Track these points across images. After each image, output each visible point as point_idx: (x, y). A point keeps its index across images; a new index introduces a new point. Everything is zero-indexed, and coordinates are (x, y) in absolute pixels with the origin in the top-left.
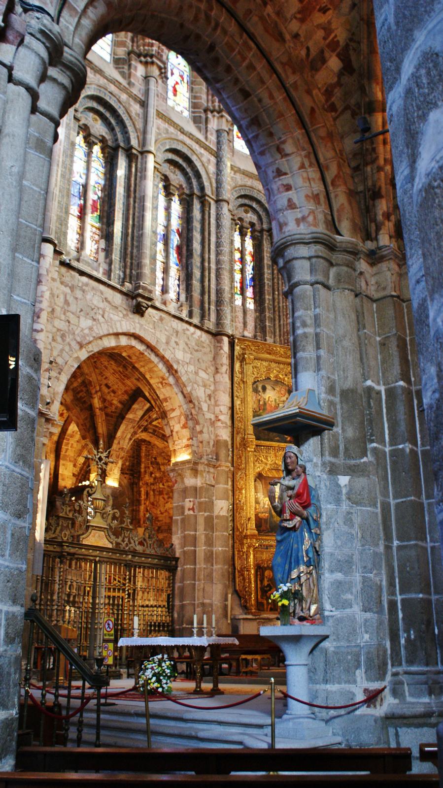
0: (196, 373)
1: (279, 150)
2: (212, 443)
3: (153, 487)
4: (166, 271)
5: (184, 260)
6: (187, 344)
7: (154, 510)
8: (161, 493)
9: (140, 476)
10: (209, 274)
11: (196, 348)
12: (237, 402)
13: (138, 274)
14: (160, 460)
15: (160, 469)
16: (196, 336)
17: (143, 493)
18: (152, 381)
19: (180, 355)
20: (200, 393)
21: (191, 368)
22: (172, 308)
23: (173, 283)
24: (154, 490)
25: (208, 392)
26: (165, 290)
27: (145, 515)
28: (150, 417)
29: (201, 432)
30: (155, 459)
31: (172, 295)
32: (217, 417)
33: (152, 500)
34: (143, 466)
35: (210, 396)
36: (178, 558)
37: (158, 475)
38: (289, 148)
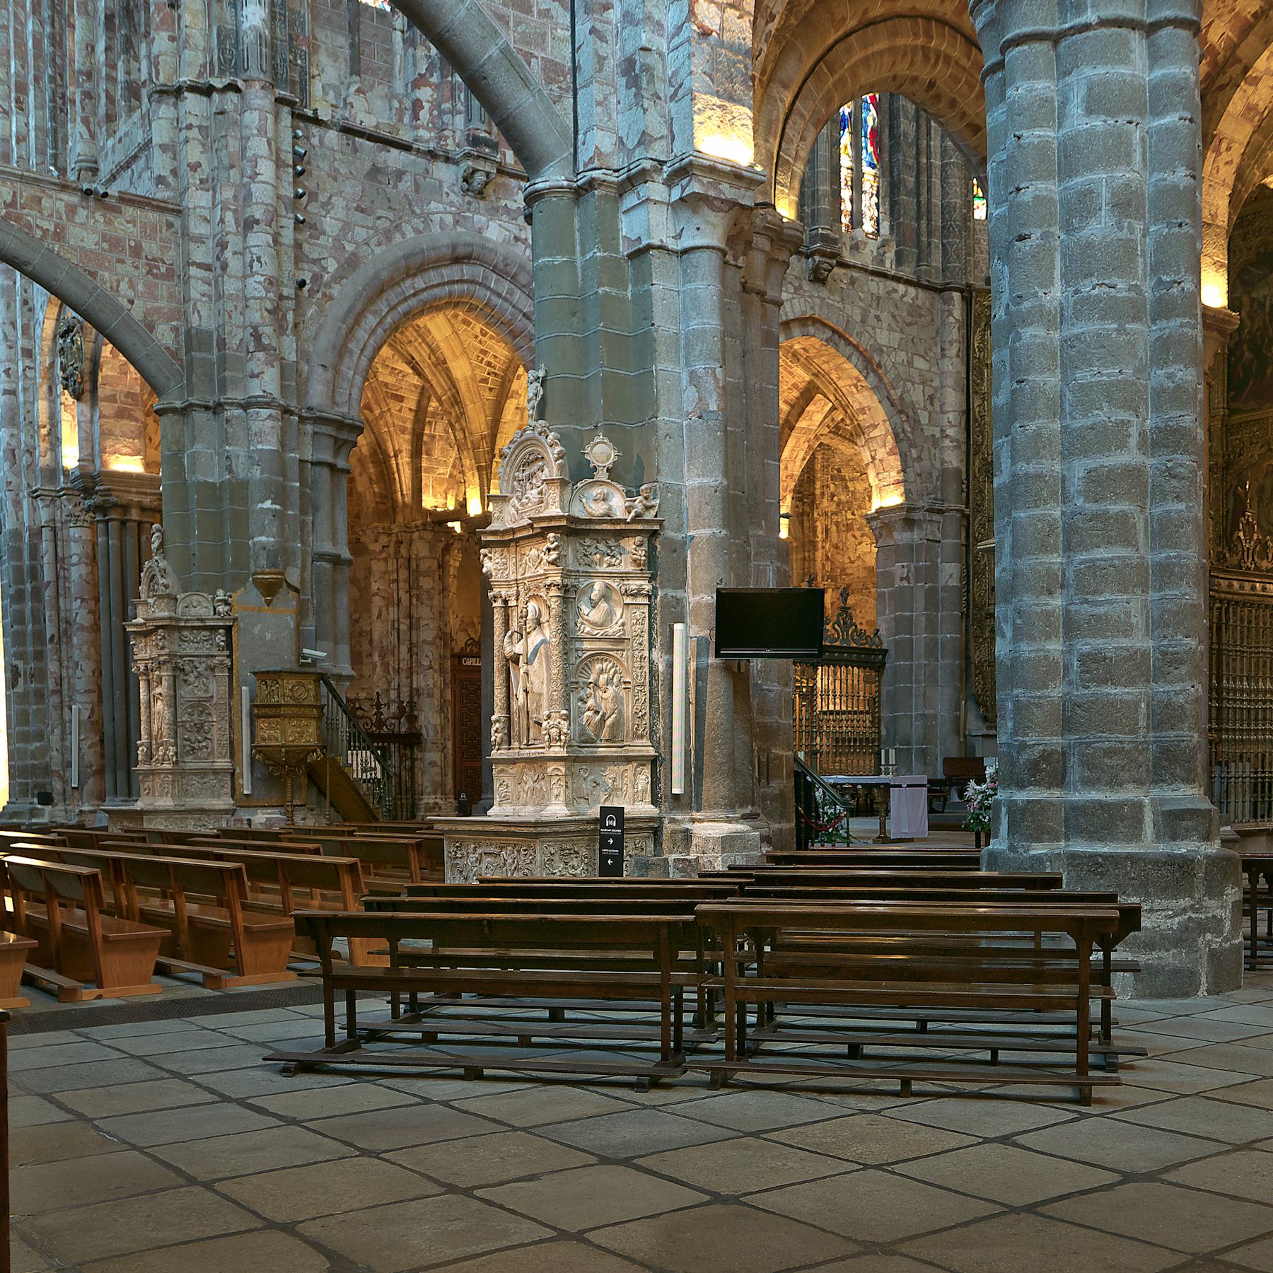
0: (910, 363)
2: (935, 474)
3: (835, 518)
4: (857, 184)
5: (886, 157)
6: (894, 317)
7: (839, 557)
8: (849, 527)
9: (813, 501)
10: (929, 177)
11: (909, 320)
12: (976, 402)
13: (813, 211)
14: (846, 473)
15: (847, 487)
16: (908, 299)
17: (819, 529)
18: (840, 384)
19: (883, 337)
20: (917, 395)
21: (902, 356)
22: (866, 258)
23: (869, 205)
24: (837, 524)
25: (929, 391)
26: (856, 221)
27: (824, 566)
28: (833, 420)
29: (919, 459)
30: (839, 471)
31: (868, 226)
32: (942, 431)
33: (835, 539)
34: (818, 485)
35: (931, 398)
36: (886, 651)
37: (843, 498)
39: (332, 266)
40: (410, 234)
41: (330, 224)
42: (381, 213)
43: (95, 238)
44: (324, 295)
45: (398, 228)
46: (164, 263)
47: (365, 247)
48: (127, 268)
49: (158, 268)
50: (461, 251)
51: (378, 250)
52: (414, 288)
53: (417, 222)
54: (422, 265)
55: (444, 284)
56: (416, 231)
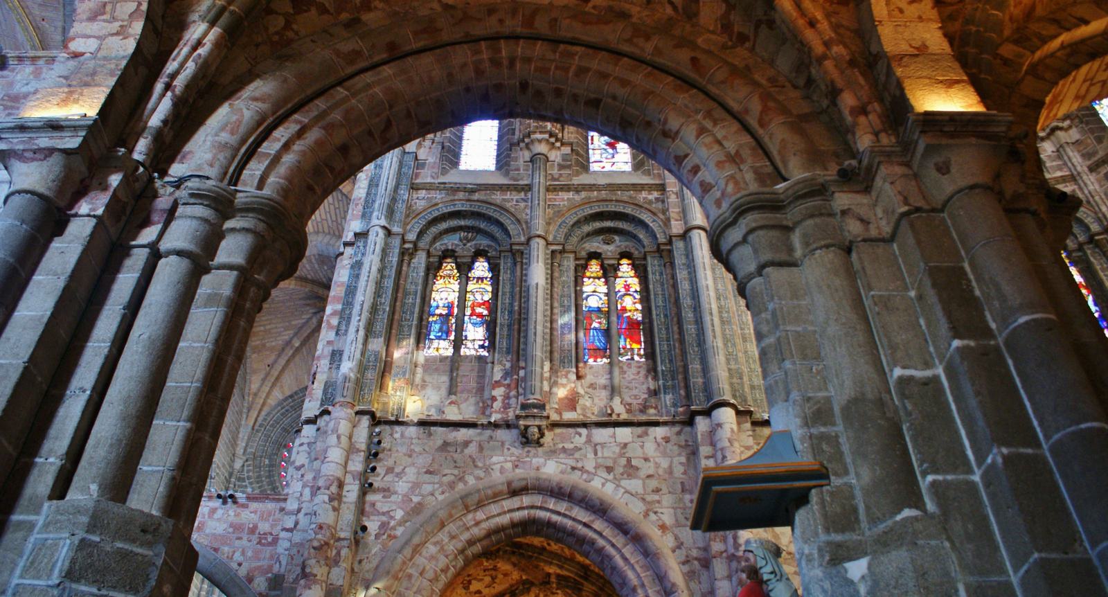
1: (666, 134)
38: (674, 123)
39: (399, 514)
40: (471, 481)
41: (402, 487)
42: (446, 471)
43: (225, 526)
44: (389, 536)
45: (461, 479)
46: (271, 534)
47: (430, 497)
48: (245, 542)
49: (266, 539)
50: (516, 485)
52: (475, 520)
53: (481, 473)
54: (479, 502)
55: (505, 513)
56: (478, 478)
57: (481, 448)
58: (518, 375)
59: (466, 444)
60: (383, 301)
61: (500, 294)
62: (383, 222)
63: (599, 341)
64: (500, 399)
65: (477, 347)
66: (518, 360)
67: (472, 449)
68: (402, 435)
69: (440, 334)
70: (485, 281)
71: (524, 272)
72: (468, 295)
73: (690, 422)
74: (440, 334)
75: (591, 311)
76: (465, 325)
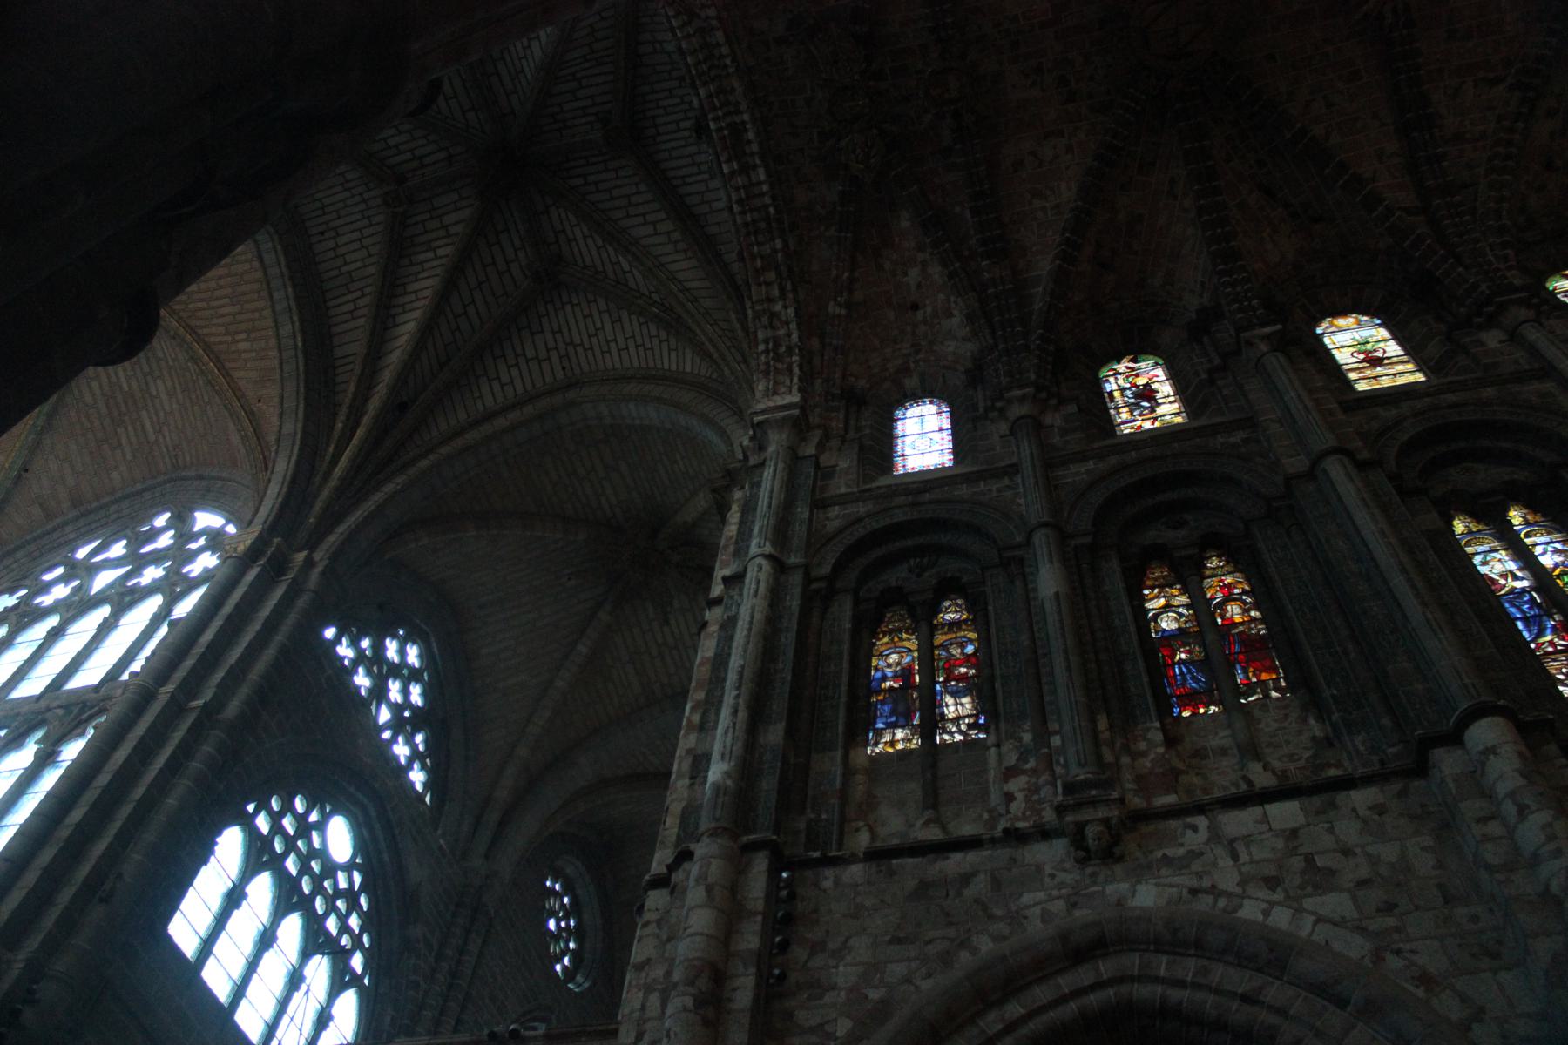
45: (964, 944)
51: (926, 985)
53: (1002, 928)
57: (996, 883)
58: (1049, 747)
59: (966, 879)
60: (780, 665)
61: (993, 631)
62: (768, 549)
63: (1196, 680)
64: (1020, 796)
65: (963, 727)
66: (1045, 722)
67: (979, 886)
68: (837, 882)
69: (893, 719)
70: (964, 627)
71: (1030, 586)
72: (936, 653)
73: (1421, 769)
74: (893, 719)
75: (1168, 637)
76: (939, 698)
